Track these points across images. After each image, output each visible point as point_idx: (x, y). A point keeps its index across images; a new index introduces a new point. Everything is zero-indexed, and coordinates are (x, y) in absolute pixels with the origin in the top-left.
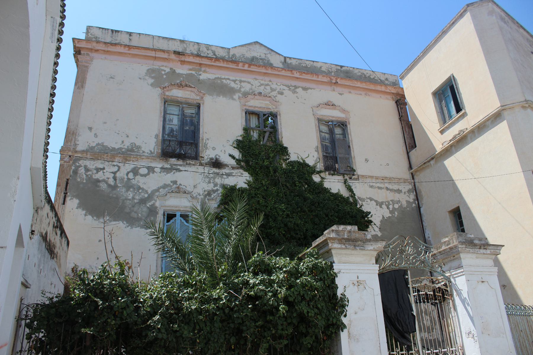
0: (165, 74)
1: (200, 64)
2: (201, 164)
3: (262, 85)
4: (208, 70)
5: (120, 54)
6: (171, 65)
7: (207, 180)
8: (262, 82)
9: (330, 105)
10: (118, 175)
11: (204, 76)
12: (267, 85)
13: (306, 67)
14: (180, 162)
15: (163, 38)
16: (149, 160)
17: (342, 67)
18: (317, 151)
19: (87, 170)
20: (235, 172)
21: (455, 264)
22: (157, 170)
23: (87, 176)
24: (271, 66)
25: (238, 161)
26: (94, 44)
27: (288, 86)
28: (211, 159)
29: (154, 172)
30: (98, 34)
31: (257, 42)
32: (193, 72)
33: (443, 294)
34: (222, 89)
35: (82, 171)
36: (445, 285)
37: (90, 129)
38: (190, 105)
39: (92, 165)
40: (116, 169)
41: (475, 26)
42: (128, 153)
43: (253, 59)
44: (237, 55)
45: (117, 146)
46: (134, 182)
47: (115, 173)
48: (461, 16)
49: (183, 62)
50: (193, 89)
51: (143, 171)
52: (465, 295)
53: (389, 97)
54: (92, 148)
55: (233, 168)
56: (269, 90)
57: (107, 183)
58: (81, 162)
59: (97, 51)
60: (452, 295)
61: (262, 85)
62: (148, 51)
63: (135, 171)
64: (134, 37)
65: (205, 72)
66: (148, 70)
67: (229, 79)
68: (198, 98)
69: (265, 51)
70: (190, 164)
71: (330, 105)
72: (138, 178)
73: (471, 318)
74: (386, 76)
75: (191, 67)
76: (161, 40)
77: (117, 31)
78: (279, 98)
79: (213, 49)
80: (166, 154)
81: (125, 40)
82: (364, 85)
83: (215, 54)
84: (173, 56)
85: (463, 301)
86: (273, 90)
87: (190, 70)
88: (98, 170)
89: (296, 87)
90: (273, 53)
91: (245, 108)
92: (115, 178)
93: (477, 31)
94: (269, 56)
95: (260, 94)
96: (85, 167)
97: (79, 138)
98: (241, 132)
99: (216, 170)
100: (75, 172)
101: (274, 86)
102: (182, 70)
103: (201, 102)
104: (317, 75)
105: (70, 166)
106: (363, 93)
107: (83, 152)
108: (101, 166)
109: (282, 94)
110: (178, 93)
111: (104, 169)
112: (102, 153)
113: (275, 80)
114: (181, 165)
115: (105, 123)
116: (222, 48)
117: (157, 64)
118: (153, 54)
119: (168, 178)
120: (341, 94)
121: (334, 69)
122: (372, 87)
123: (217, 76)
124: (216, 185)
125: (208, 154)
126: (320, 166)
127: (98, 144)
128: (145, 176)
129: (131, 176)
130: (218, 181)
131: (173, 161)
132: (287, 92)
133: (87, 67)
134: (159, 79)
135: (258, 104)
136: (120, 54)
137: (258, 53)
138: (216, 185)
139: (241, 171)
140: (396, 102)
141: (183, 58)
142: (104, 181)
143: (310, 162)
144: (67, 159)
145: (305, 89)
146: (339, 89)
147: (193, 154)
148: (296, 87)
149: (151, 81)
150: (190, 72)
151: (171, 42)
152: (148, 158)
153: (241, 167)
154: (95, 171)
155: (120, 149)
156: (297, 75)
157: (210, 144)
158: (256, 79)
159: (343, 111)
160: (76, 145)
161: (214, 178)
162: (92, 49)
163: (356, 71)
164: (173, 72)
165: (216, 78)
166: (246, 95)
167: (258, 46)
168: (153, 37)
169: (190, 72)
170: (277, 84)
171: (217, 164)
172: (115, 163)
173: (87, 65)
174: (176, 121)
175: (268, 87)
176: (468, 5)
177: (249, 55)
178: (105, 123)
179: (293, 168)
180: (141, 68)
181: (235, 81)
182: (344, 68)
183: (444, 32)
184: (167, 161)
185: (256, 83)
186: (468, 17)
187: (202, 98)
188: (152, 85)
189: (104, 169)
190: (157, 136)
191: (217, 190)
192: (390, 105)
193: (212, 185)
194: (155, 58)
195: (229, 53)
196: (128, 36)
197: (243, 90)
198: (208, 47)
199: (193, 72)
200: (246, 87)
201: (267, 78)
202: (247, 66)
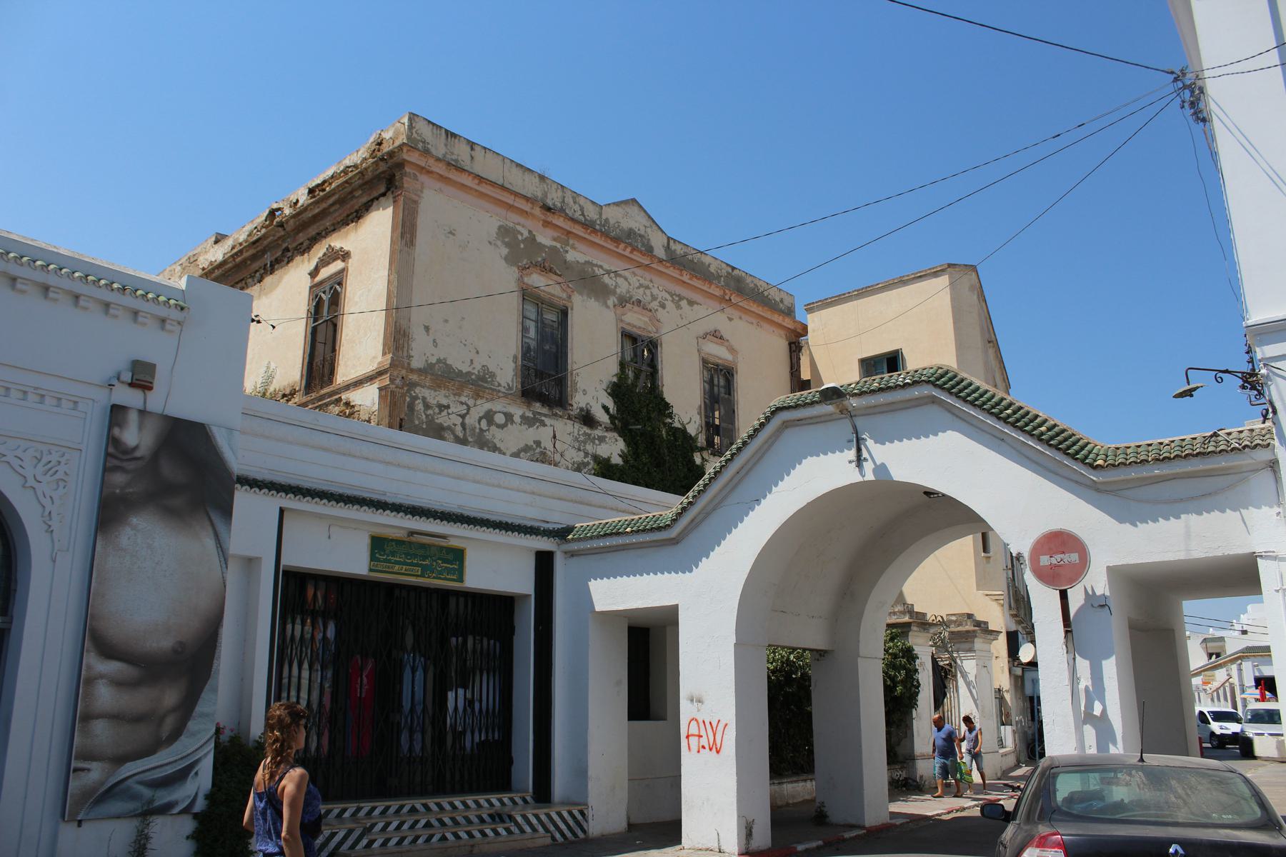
0: (523, 241)
1: (569, 233)
2: (569, 418)
3: (641, 286)
4: (577, 244)
5: (463, 187)
6: (530, 223)
7: (576, 445)
8: (642, 281)
9: (716, 336)
10: (467, 420)
11: (572, 256)
12: (647, 287)
13: (692, 261)
14: (545, 411)
15: (518, 165)
16: (508, 401)
17: (733, 268)
18: (700, 413)
19: (427, 406)
20: (609, 435)
21: (966, 646)
22: (517, 419)
23: (427, 416)
24: (649, 250)
25: (612, 417)
26: (431, 161)
27: (671, 295)
28: (582, 409)
29: (512, 422)
30: (426, 132)
31: (634, 201)
32: (558, 245)
33: (946, 674)
34: (591, 284)
35: (419, 406)
36: (950, 665)
37: (427, 328)
38: (551, 305)
39: (436, 397)
40: (463, 409)
41: (953, 300)
42: (480, 384)
43: (631, 233)
44: (612, 221)
45: (465, 369)
46: (488, 436)
47: (463, 417)
48: (936, 274)
49: (547, 224)
50: (559, 279)
51: (500, 419)
52: (971, 677)
53: (782, 333)
54: (431, 366)
55: (607, 429)
56: (649, 298)
57: (453, 432)
58: (418, 390)
59: (429, 172)
60: (955, 676)
61: (641, 286)
62: (505, 194)
63: (489, 416)
64: (478, 153)
65: (573, 248)
66: (500, 227)
67: (601, 267)
68: (564, 296)
69: (645, 221)
70: (556, 415)
71: (716, 336)
72: (493, 428)
73: (975, 701)
74: (783, 295)
75: (556, 234)
76: (515, 170)
77: (454, 135)
78: (661, 314)
79: (582, 201)
80: (529, 394)
81: (461, 152)
82: (754, 308)
83: (583, 214)
84: (537, 211)
85: (968, 684)
86: (654, 298)
87: (555, 239)
88: (442, 407)
89: (681, 298)
90: (654, 227)
91: (621, 325)
92: (463, 425)
93: (953, 307)
94: (649, 230)
95: (639, 302)
96: (424, 399)
97: (413, 345)
98: (615, 369)
99: (586, 429)
100: (411, 407)
101: (655, 291)
102: (545, 238)
103: (569, 305)
104: (711, 283)
105: (403, 396)
106: (755, 321)
107: (420, 371)
108: (445, 402)
109: (663, 306)
110: (537, 280)
111: (448, 407)
112: (443, 375)
113: (658, 281)
114: (545, 415)
115: (446, 321)
116: (593, 203)
117: (513, 219)
118: (510, 199)
119: (531, 435)
120: (730, 319)
121: (724, 273)
122: (768, 315)
123: (587, 258)
124: (586, 454)
125: (579, 401)
126: (701, 440)
127: (439, 361)
128: (501, 427)
129: (484, 424)
130: (589, 448)
131: (537, 406)
132: (669, 305)
133: (416, 202)
134: (524, 255)
135: (636, 320)
136: (463, 187)
137: (634, 221)
138: (586, 454)
139: (616, 435)
140: (790, 344)
141: (551, 218)
142: (449, 428)
143: (692, 430)
144: (398, 381)
145: (691, 303)
146: (729, 310)
147: (554, 393)
148: (681, 298)
149: (505, 251)
150: (554, 244)
151: (527, 176)
152: (506, 396)
153: (614, 428)
154: (437, 410)
155: (469, 373)
156: (686, 278)
157: (581, 385)
158: (635, 274)
159: (732, 350)
160: (410, 357)
161: (585, 442)
162: (423, 168)
163: (749, 280)
164: (532, 239)
165: (587, 263)
166: (623, 301)
167: (636, 208)
168: (504, 158)
169: (554, 244)
170: (660, 288)
171: (587, 419)
172: (463, 399)
173: (416, 198)
174: (532, 333)
175: (648, 292)
176: (950, 265)
177: (627, 224)
178: (446, 321)
179: (676, 439)
180: (487, 221)
181: (608, 272)
182: (736, 272)
183: (903, 282)
184: (529, 405)
185: (634, 280)
186: (944, 280)
187: (570, 297)
188: (506, 259)
189: (448, 407)
190: (515, 357)
191: (588, 463)
192: (780, 345)
193: (582, 454)
194: (510, 207)
195: (601, 214)
196: (468, 148)
197: (618, 291)
198: (576, 196)
199: (558, 245)
200: (623, 288)
201: (648, 275)
202: (629, 249)
